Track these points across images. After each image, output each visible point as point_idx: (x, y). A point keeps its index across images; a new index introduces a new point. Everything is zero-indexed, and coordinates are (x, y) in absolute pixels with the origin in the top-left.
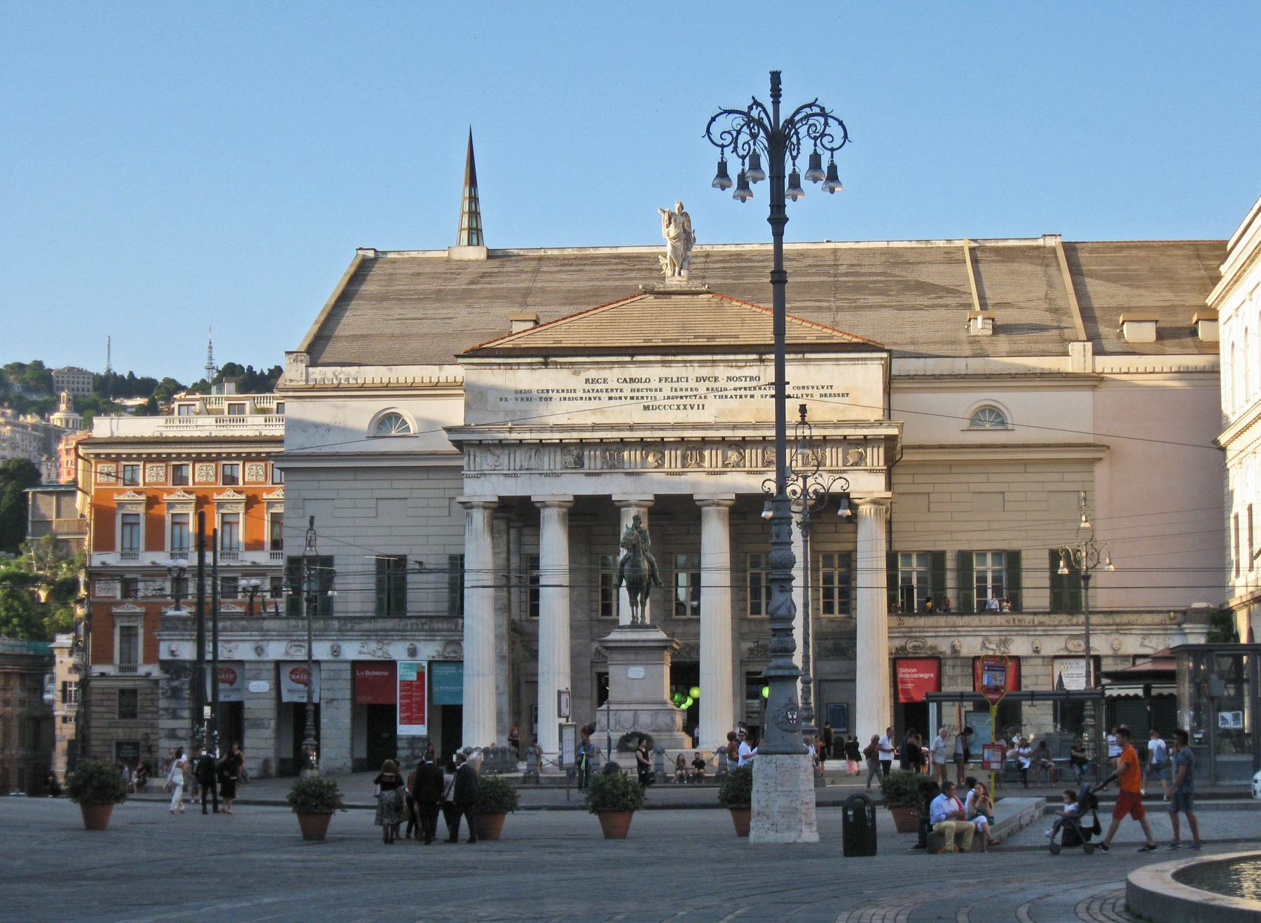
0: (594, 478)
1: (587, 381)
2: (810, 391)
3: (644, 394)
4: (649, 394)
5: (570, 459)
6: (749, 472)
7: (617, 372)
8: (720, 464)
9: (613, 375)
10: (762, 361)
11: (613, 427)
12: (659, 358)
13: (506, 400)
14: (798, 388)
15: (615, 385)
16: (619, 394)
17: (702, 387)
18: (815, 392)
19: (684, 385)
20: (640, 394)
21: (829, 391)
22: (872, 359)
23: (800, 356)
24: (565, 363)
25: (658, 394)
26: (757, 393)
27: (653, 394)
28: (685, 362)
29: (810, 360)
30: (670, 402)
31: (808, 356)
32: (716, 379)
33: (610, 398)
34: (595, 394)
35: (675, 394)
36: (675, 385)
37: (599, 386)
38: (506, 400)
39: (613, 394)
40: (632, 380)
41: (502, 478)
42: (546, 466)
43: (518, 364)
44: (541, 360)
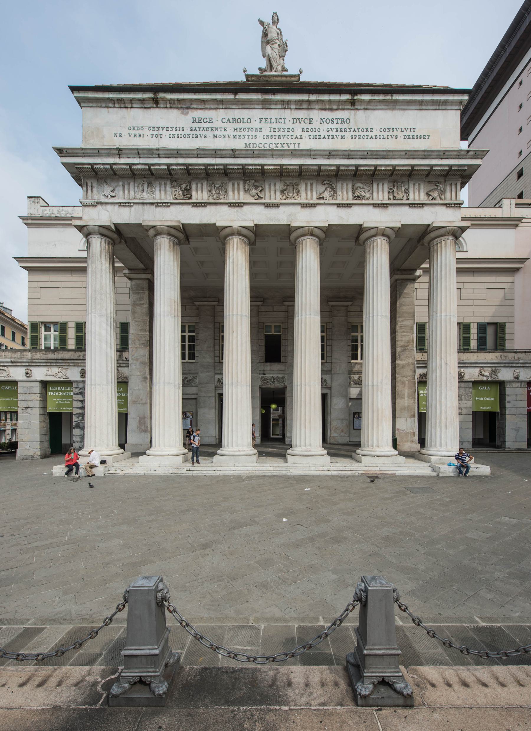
0: (201, 209)
2: (395, 133)
3: (246, 133)
4: (250, 133)
6: (339, 205)
7: (222, 114)
9: (218, 116)
10: (353, 103)
11: (216, 153)
13: (120, 136)
15: (219, 124)
16: (223, 133)
17: (298, 127)
18: (399, 133)
19: (282, 126)
20: (242, 133)
21: (412, 134)
22: (452, 103)
23: (388, 97)
24: (173, 100)
25: (258, 134)
26: (348, 134)
27: (254, 133)
28: (282, 102)
29: (396, 102)
31: (396, 97)
32: (311, 121)
33: (215, 137)
34: (201, 133)
35: (273, 133)
36: (274, 126)
38: (120, 136)
39: (218, 133)
40: (235, 121)
41: (117, 207)
43: (131, 100)
44: (150, 95)
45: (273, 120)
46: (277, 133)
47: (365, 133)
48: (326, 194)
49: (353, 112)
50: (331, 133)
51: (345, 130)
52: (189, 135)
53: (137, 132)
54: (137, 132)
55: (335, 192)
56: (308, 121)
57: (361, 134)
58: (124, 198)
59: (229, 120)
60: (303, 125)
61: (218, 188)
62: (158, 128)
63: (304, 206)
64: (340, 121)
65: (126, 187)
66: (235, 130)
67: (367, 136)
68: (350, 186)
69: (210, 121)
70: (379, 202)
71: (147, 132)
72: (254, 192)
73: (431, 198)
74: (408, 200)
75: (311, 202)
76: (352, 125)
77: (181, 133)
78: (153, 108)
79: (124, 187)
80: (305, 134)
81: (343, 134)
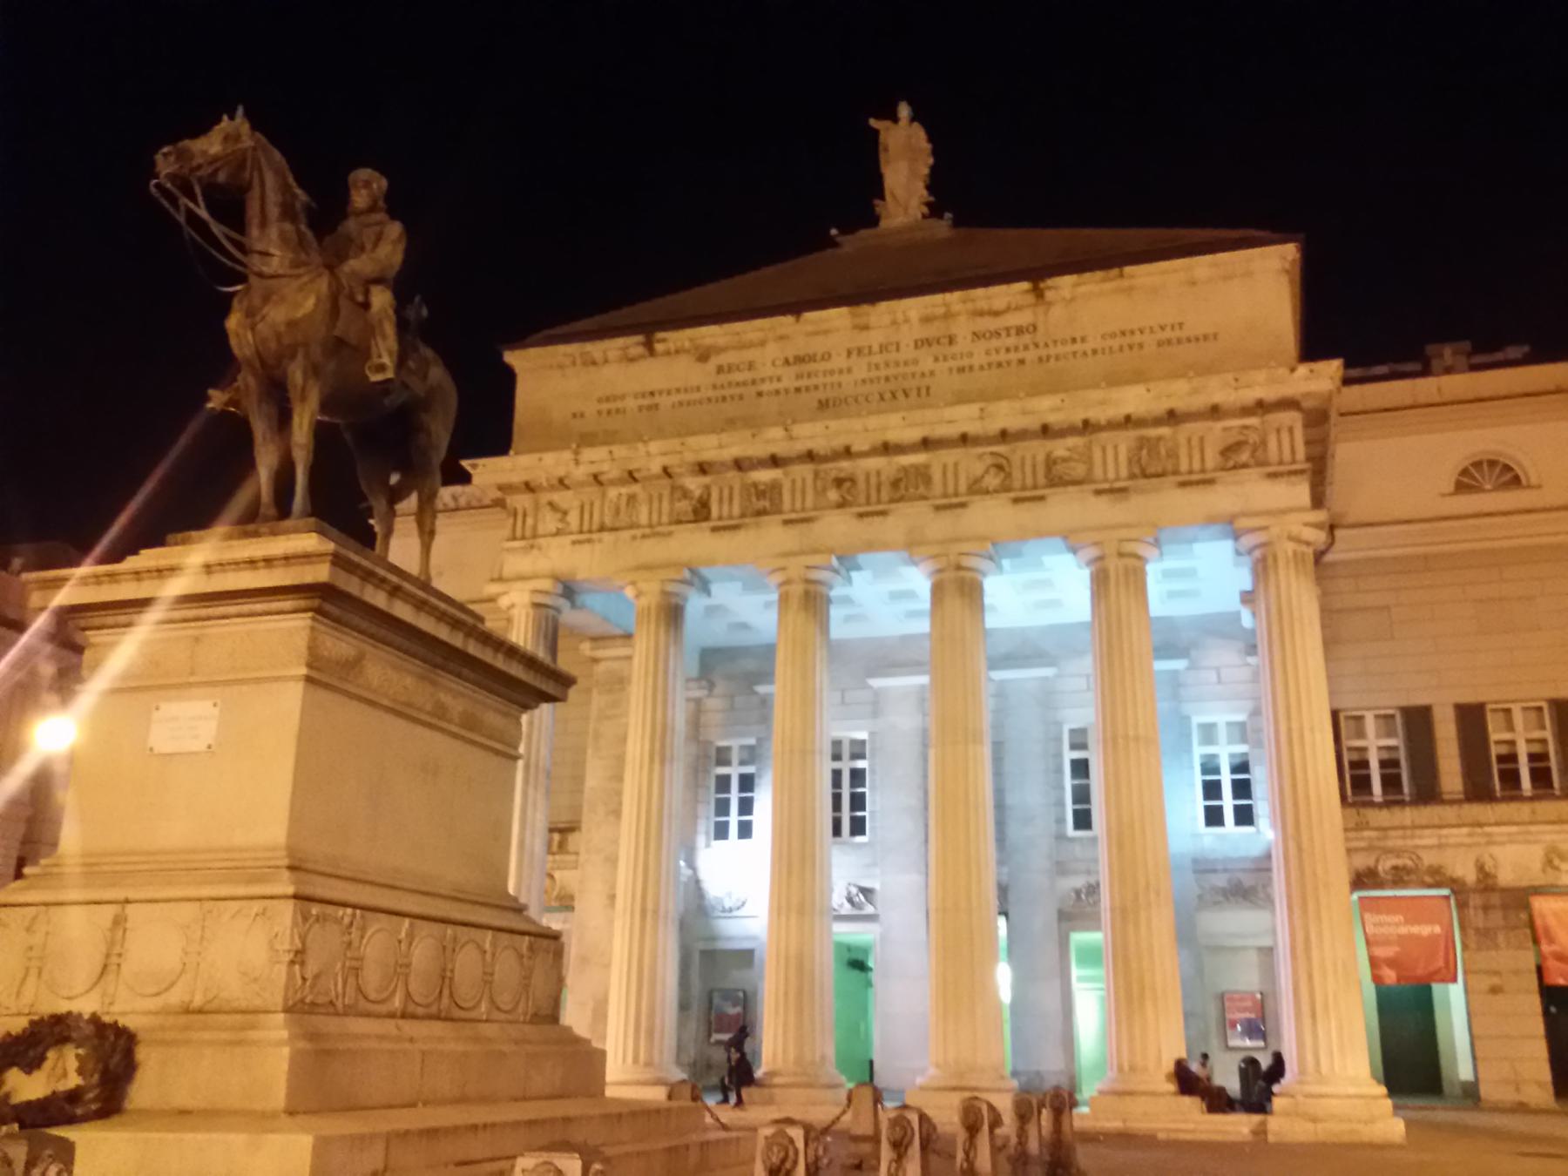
0: (727, 535)
1: (720, 370)
4: (829, 379)
5: (684, 506)
7: (773, 350)
8: (963, 488)
10: (1039, 293)
12: (844, 310)
14: (1113, 335)
15: (768, 371)
16: (776, 385)
18: (1147, 338)
19: (893, 356)
21: (1178, 333)
23: (1115, 271)
25: (845, 379)
26: (1031, 355)
27: (836, 378)
30: (867, 388)
31: (1128, 270)
32: (951, 340)
33: (760, 394)
35: (874, 374)
36: (877, 359)
37: (738, 377)
38: (582, 415)
39: (766, 387)
40: (800, 360)
42: (644, 519)
45: (876, 348)
46: (883, 373)
47: (1070, 348)
48: (993, 481)
49: (1041, 310)
50: (994, 358)
51: (1026, 348)
52: (709, 400)
53: (612, 406)
54: (612, 406)
55: (1009, 475)
56: (946, 341)
57: (1060, 349)
58: (581, 532)
59: (787, 362)
60: (935, 349)
61: (761, 494)
62: (652, 394)
63: (938, 508)
64: (1013, 332)
65: (587, 508)
66: (799, 377)
67: (1074, 353)
68: (1041, 458)
69: (751, 366)
70: (1106, 486)
71: (631, 404)
72: (833, 495)
73: (1231, 463)
74: (1176, 472)
75: (955, 500)
76: (1040, 337)
77: (696, 396)
78: (641, 357)
79: (582, 508)
80: (942, 366)
81: (1021, 355)
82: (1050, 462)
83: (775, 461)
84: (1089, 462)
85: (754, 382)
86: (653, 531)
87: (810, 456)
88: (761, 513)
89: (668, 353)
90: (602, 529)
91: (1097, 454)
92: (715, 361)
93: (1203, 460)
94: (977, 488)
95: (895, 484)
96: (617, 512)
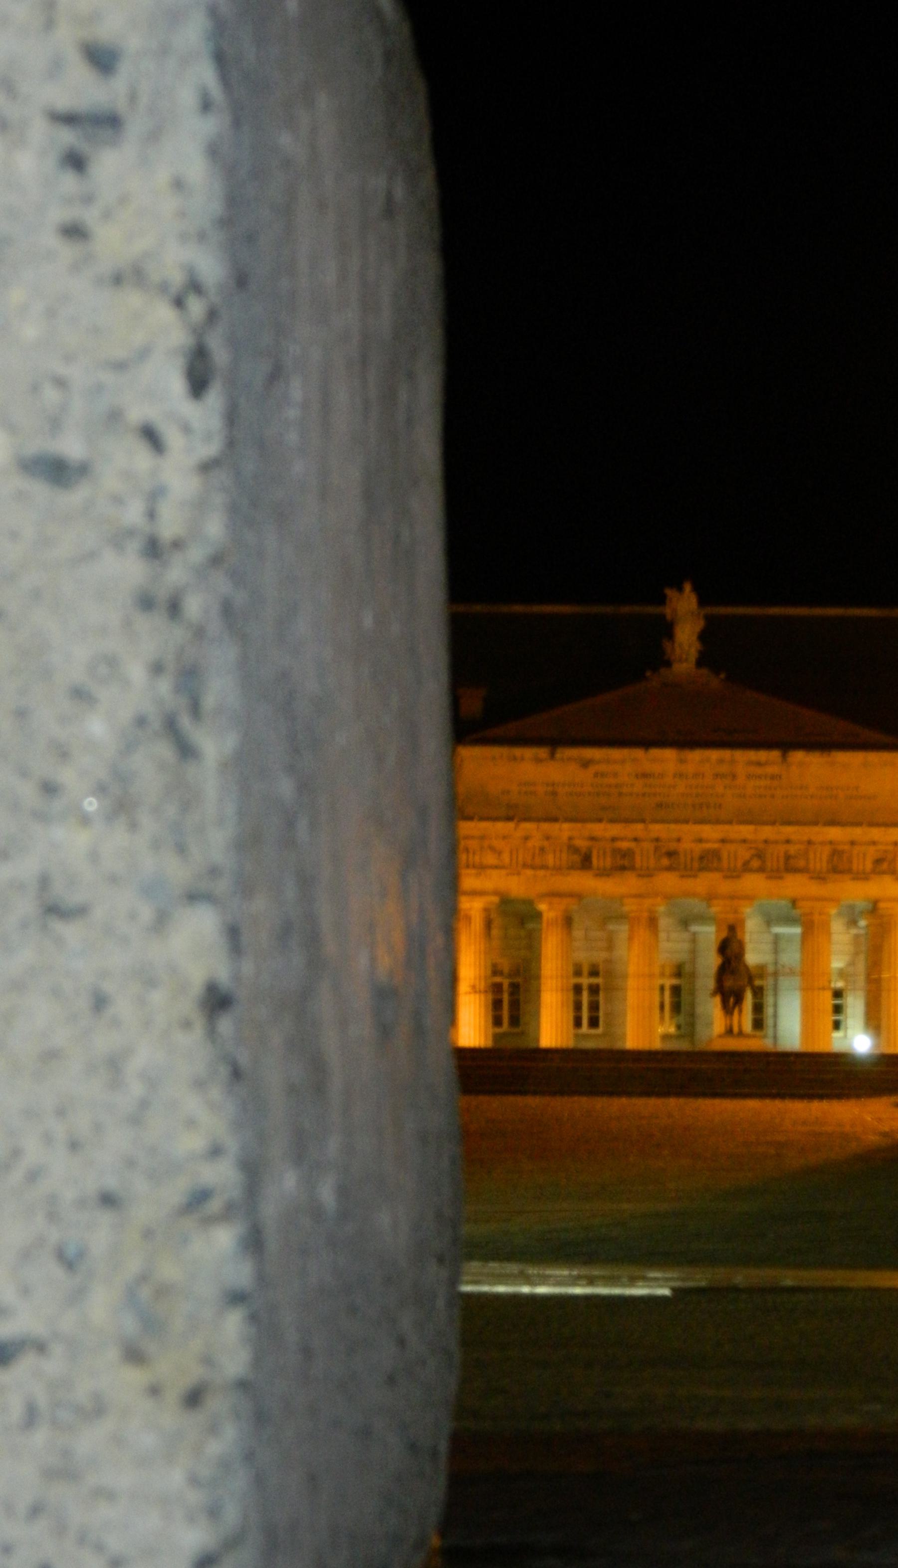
10: (784, 756)
32: (734, 777)
33: (620, 794)
39: (625, 790)
40: (645, 775)
48: (755, 864)
55: (764, 862)
61: (624, 856)
82: (788, 857)
83: (636, 840)
84: (807, 860)
85: (616, 786)
86: (558, 869)
87: (657, 840)
88: (623, 868)
89: (562, 760)
90: (525, 866)
91: (811, 856)
92: (592, 769)
93: (864, 865)
94: (746, 868)
95: (701, 858)
96: (533, 858)
